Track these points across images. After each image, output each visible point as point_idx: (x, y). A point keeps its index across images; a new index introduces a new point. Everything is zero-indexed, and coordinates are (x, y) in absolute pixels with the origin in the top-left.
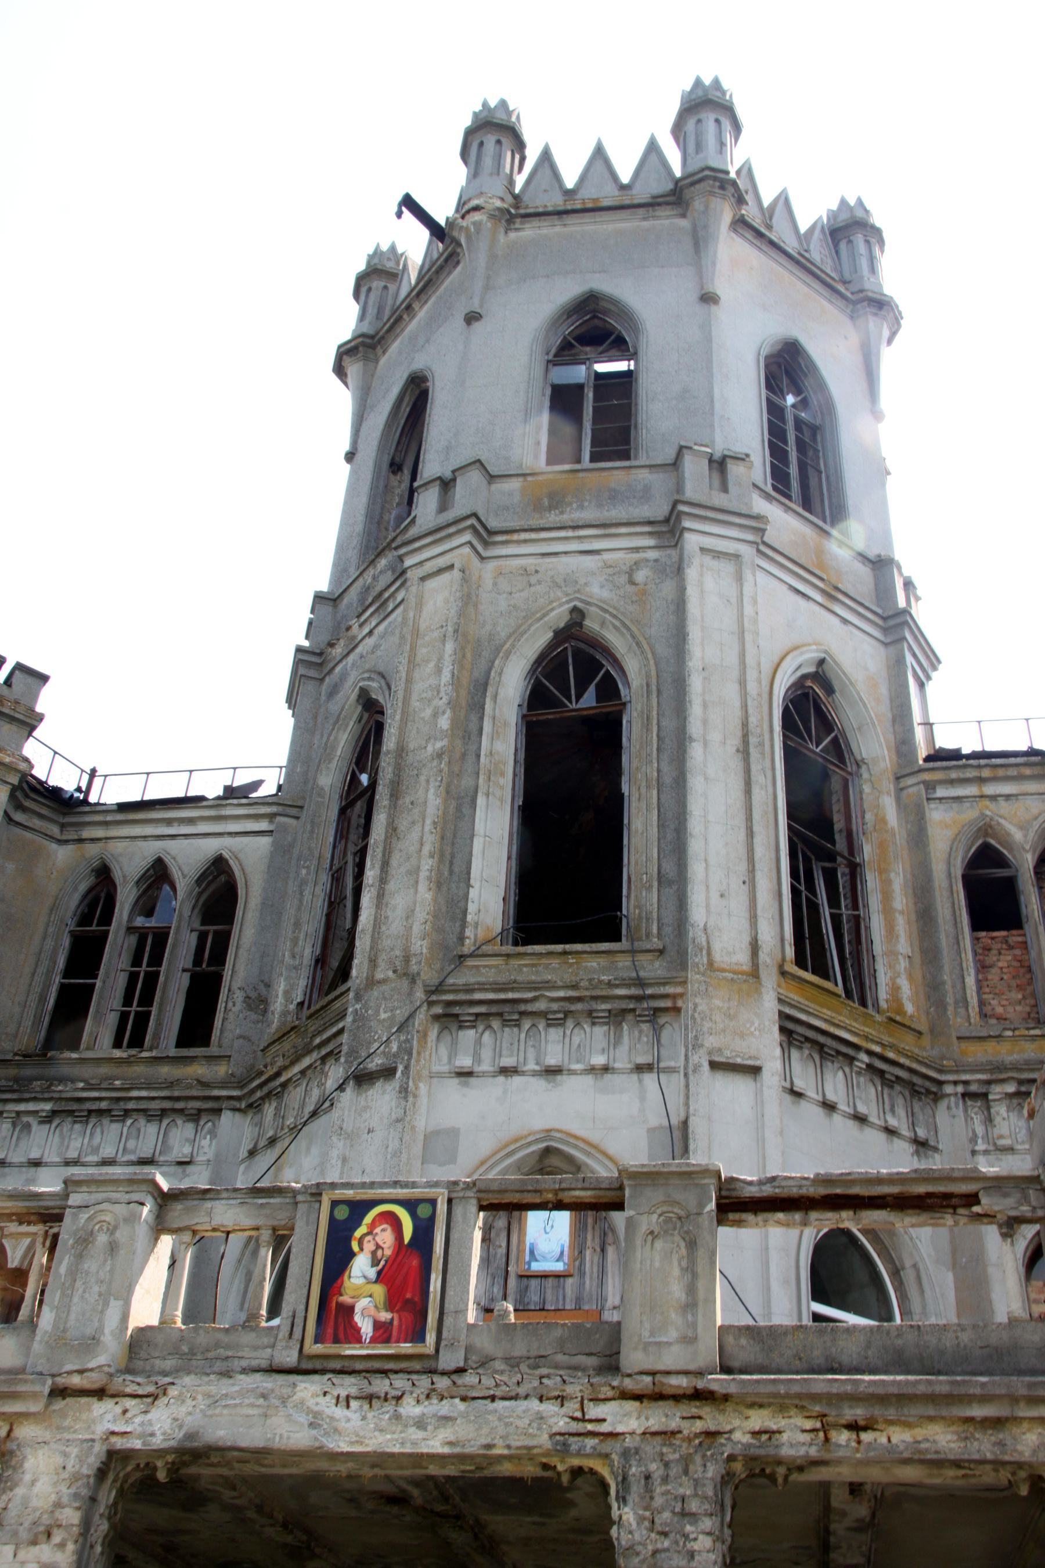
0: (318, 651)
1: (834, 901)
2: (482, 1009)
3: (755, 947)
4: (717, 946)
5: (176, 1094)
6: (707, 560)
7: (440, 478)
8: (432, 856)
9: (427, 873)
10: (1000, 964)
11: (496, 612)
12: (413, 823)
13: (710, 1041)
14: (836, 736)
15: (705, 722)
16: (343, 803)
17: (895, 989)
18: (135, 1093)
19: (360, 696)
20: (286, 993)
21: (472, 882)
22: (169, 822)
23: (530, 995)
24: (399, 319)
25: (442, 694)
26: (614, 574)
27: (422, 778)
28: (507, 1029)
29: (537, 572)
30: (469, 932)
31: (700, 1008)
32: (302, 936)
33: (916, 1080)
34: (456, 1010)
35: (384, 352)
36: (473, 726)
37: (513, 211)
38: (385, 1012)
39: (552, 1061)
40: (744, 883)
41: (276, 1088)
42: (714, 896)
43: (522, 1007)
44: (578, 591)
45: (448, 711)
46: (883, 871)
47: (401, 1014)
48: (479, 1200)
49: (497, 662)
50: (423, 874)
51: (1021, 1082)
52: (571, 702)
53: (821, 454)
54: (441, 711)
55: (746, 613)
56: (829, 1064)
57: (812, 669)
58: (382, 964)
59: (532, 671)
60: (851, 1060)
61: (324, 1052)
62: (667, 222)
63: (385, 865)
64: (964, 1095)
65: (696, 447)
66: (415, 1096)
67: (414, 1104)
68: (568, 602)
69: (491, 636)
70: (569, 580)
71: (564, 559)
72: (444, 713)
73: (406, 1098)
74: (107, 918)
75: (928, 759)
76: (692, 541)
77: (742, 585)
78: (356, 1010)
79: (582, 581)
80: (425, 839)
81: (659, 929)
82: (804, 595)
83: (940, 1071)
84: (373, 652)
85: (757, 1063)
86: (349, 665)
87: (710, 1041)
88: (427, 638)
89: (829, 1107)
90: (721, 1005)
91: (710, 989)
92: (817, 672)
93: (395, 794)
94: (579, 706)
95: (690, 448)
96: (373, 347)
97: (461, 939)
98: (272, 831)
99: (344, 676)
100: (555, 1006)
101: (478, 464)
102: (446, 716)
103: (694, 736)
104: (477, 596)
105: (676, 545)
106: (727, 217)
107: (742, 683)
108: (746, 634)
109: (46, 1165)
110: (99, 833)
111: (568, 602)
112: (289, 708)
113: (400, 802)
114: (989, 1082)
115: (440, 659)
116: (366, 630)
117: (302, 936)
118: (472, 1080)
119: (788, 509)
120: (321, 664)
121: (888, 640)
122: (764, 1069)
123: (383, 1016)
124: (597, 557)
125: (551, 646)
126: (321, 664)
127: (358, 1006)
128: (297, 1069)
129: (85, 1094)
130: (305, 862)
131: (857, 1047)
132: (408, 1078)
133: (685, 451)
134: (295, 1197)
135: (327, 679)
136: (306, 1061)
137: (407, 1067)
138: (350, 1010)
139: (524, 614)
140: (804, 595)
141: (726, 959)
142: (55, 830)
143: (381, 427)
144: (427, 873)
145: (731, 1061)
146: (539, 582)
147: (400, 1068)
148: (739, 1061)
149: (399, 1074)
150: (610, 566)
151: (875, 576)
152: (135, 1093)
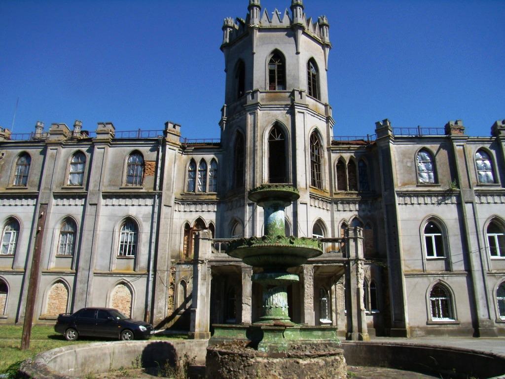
1: (317, 171)
30: (263, 181)
46: (325, 166)
60: (319, 199)
69: (263, 126)
70: (275, 115)
89: (315, 207)
106: (302, 32)
116: (237, 117)
119: (311, 98)
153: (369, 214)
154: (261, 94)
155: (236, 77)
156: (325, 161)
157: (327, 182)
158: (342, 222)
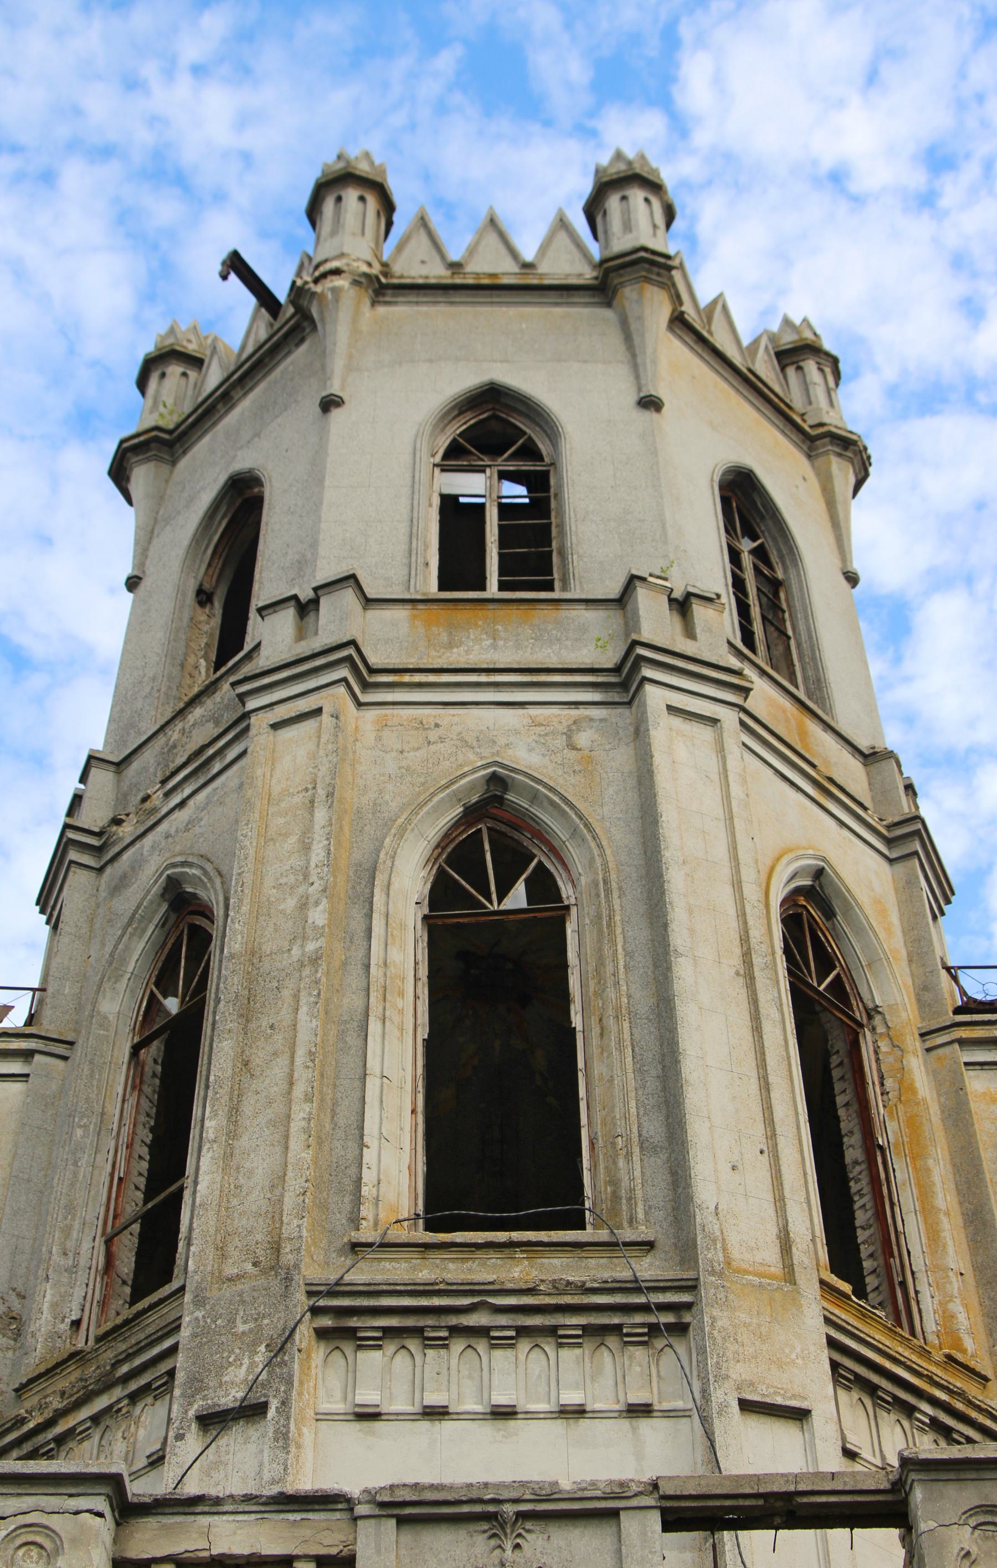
0: (97, 830)
2: (393, 1322)
3: (786, 1244)
4: (733, 1239)
6: (677, 722)
7: (295, 597)
8: (308, 1099)
9: (303, 1123)
11: (383, 775)
12: (275, 1054)
13: (738, 1371)
14: (838, 975)
15: (692, 931)
16: (136, 1040)
17: (948, 1318)
19: (166, 890)
20: (54, 1305)
21: (366, 1139)
25: (313, 878)
26: (546, 734)
27: (286, 993)
28: (430, 1353)
29: (437, 725)
30: (366, 1211)
31: (719, 1323)
32: (77, 1225)
34: (354, 1322)
35: (185, 453)
36: (358, 926)
37: (383, 280)
38: (245, 1322)
39: (501, 1398)
40: (762, 1152)
41: (48, 1443)
42: (725, 1168)
44: (498, 753)
45: (324, 902)
46: (917, 1155)
47: (272, 1326)
48: (664, 1512)
49: (388, 841)
50: (297, 1125)
52: (491, 903)
53: (787, 615)
54: (312, 900)
55: (733, 794)
56: (885, 1414)
57: (807, 882)
58: (234, 1254)
59: (432, 859)
60: (909, 1411)
61: (133, 1386)
63: (234, 1111)
65: (650, 579)
66: (299, 1446)
67: (297, 1457)
69: (376, 807)
72: (317, 903)
73: (286, 1448)
76: (655, 697)
77: (724, 758)
78: (197, 1319)
79: (502, 741)
80: (296, 1076)
81: (646, 1213)
82: (792, 784)
84: (187, 830)
86: (146, 848)
87: (738, 1371)
88: (283, 805)
90: (748, 1320)
91: (731, 1297)
92: (812, 886)
94: (502, 907)
95: (643, 579)
97: (355, 1221)
98: (27, 1075)
99: (137, 866)
101: (352, 581)
102: (321, 907)
103: (680, 949)
104: (355, 752)
105: (629, 703)
106: (665, 312)
107: (737, 885)
108: (736, 820)
112: (42, 911)
113: (252, 1026)
115: (307, 831)
117: (77, 1225)
118: (378, 1425)
121: (894, 855)
122: (813, 1413)
123: (241, 1327)
124: (520, 712)
127: (200, 1314)
128: (85, 1412)
130: (81, 1119)
132: (288, 1418)
133: (638, 583)
134: (352, 1510)
135: (109, 870)
136: (102, 1402)
137: (284, 1403)
138: (186, 1319)
139: (422, 780)
140: (792, 784)
143: (186, 543)
144: (303, 1123)
145: (768, 1400)
146: (442, 740)
147: (274, 1404)
148: (779, 1400)
149: (271, 1413)
150: (541, 725)
151: (868, 774)
154: (378, 615)
155: (203, 597)
156: (914, 1124)
157: (955, 1284)
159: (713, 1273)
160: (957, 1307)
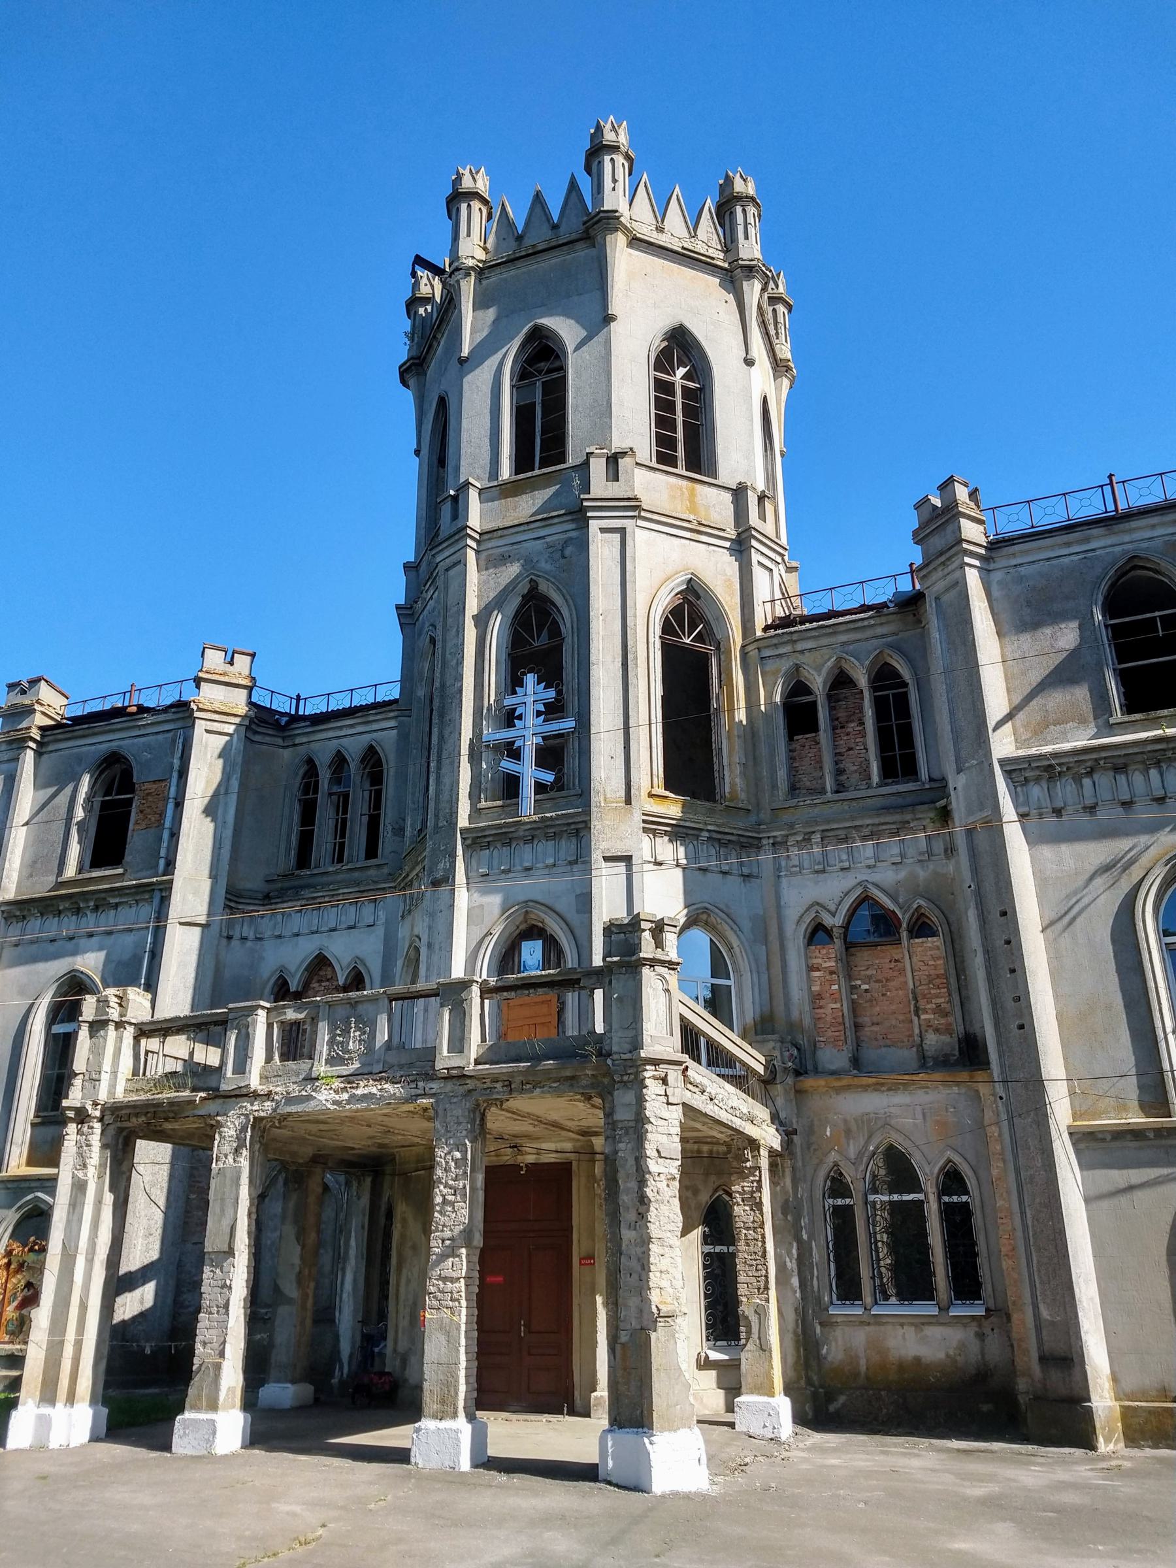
5: (362, 889)
10: (810, 755)
17: (733, 785)
18: (341, 891)
22: (341, 728)
23: (512, 829)
24: (430, 346)
33: (742, 839)
39: (527, 864)
43: (510, 836)
51: (805, 834)
59: (512, 624)
62: (582, 253)
64: (773, 844)
68: (527, 576)
71: (525, 545)
74: (316, 791)
75: (766, 628)
76: (594, 525)
79: (535, 560)
83: (759, 833)
85: (630, 854)
93: (442, 716)
96: (421, 365)
100: (527, 833)
106: (621, 239)
109: (303, 935)
110: (304, 740)
111: (527, 576)
114: (787, 836)
120: (412, 614)
123: (442, 848)
125: (522, 606)
126: (412, 614)
129: (316, 895)
131: (701, 830)
141: (613, 796)
142: (280, 741)
152: (341, 891)
153: (922, 874)
158: (808, 919)
159: (597, 807)
160: (738, 780)
